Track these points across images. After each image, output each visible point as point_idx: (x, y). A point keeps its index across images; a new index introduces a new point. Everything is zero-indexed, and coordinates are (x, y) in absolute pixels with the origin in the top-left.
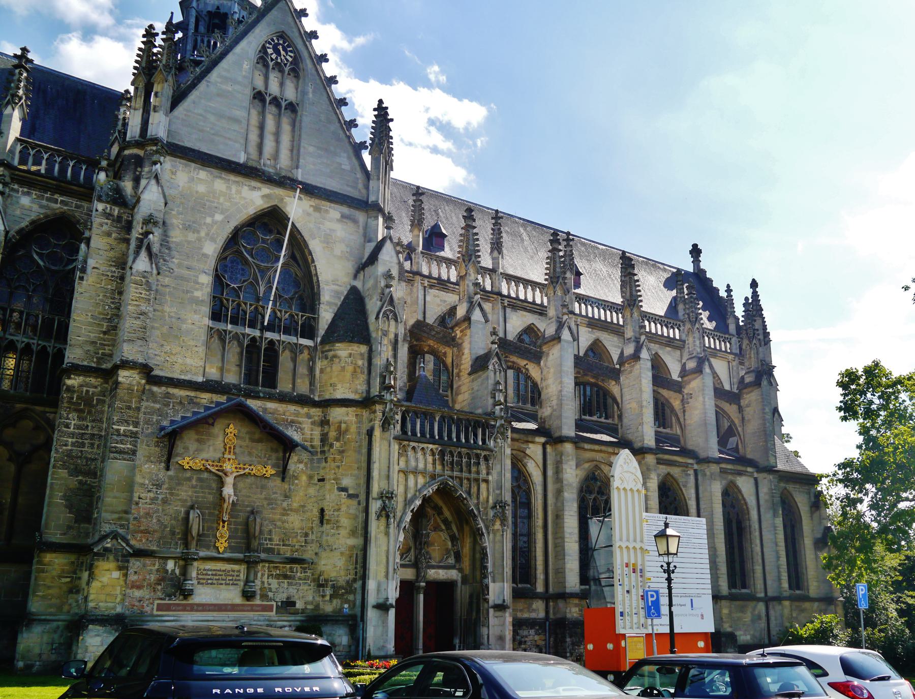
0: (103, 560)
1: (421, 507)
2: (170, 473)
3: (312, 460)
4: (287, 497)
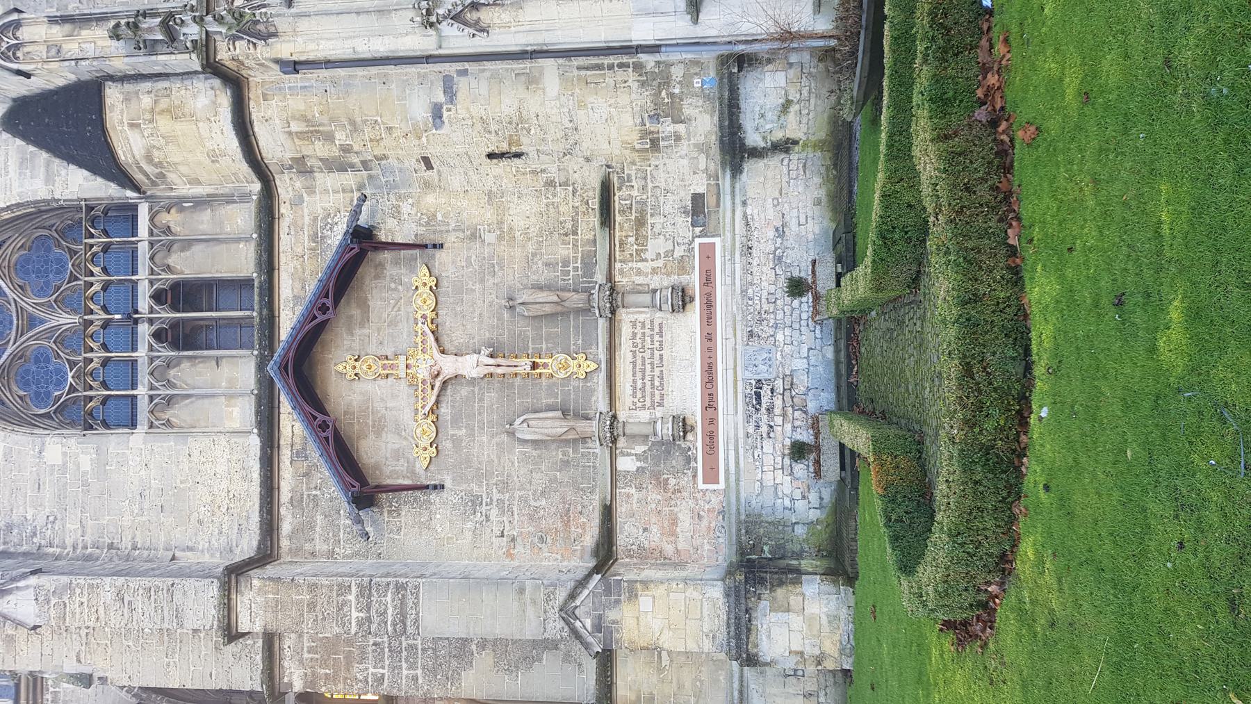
0: (618, 631)
2: (448, 484)
3: (392, 186)
4: (474, 236)
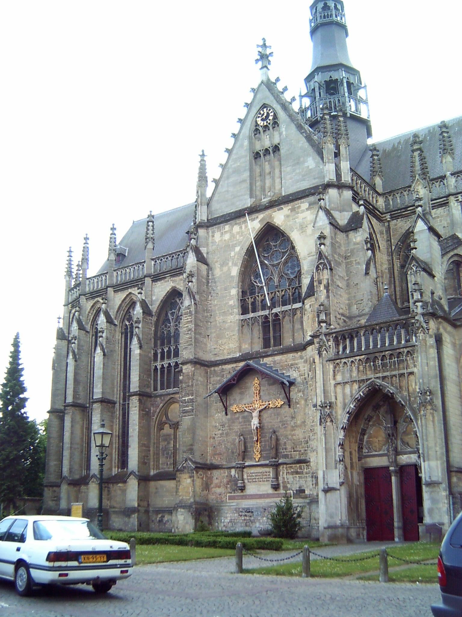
2: (229, 416)
4: (293, 418)
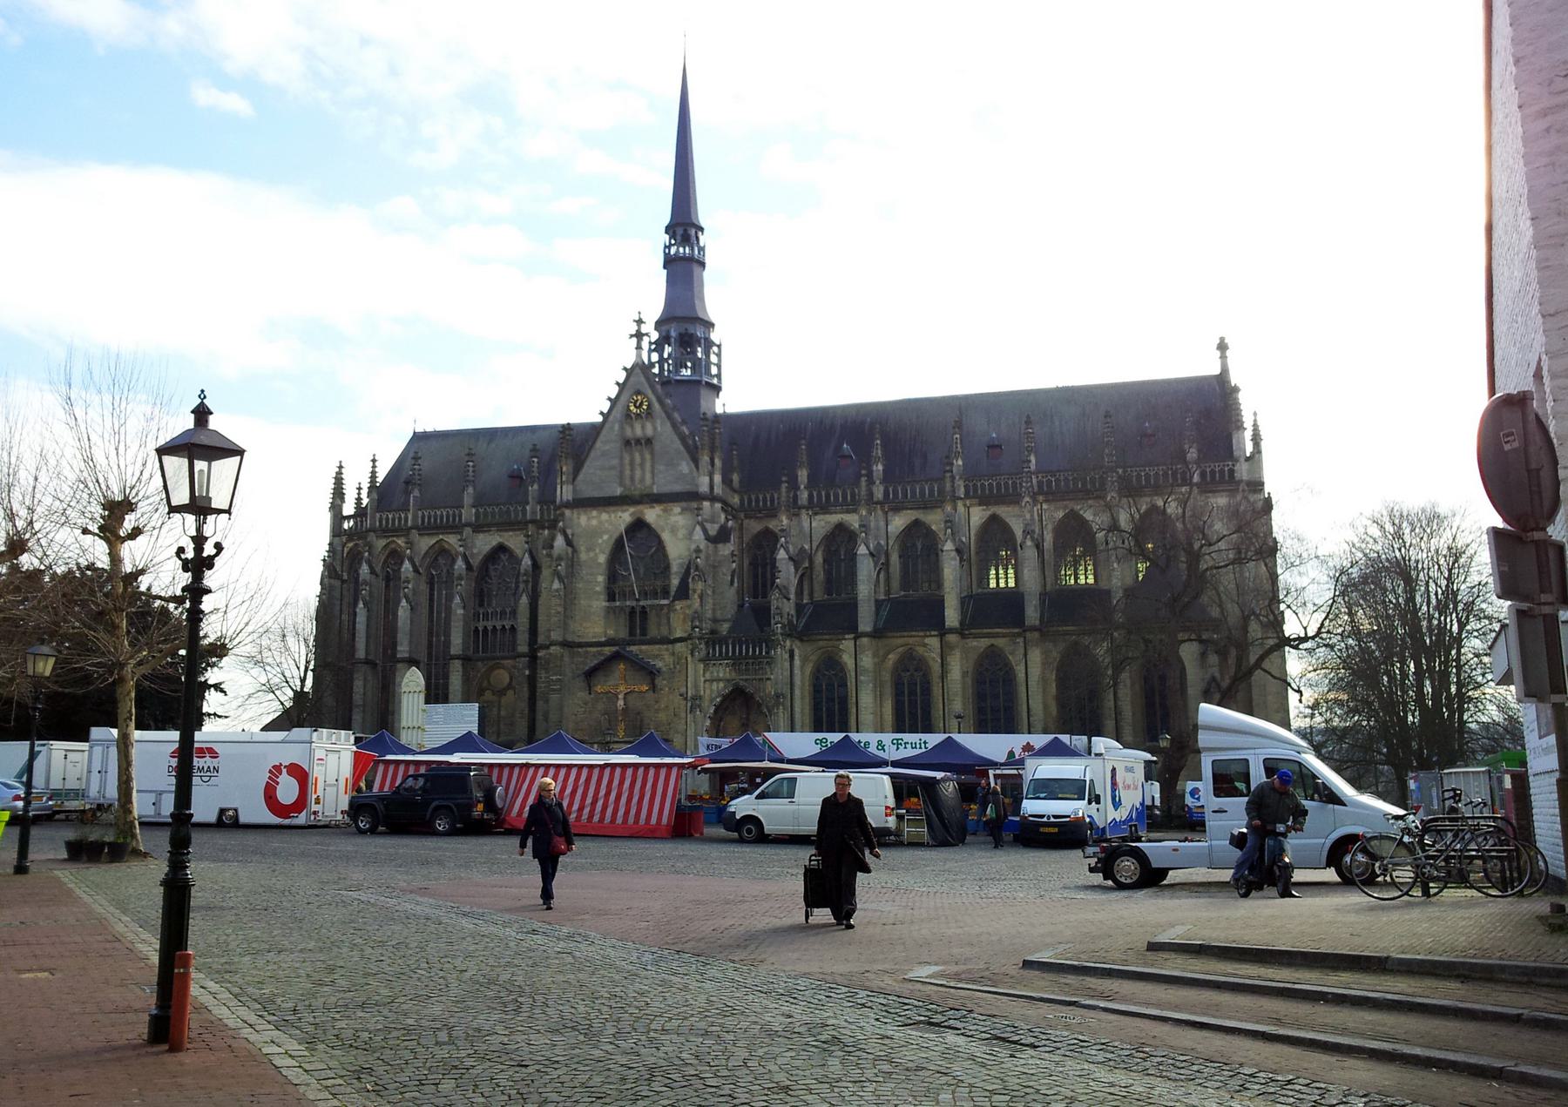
1: (722, 702)
4: (657, 702)
